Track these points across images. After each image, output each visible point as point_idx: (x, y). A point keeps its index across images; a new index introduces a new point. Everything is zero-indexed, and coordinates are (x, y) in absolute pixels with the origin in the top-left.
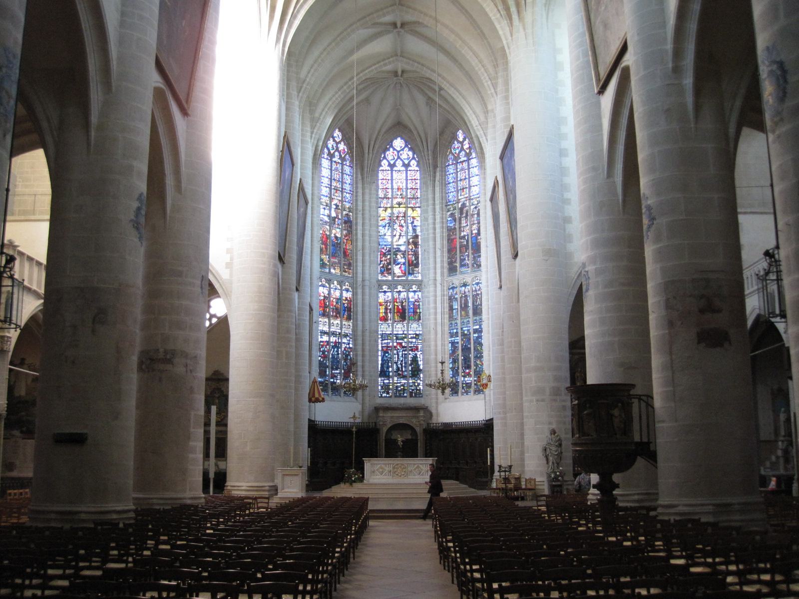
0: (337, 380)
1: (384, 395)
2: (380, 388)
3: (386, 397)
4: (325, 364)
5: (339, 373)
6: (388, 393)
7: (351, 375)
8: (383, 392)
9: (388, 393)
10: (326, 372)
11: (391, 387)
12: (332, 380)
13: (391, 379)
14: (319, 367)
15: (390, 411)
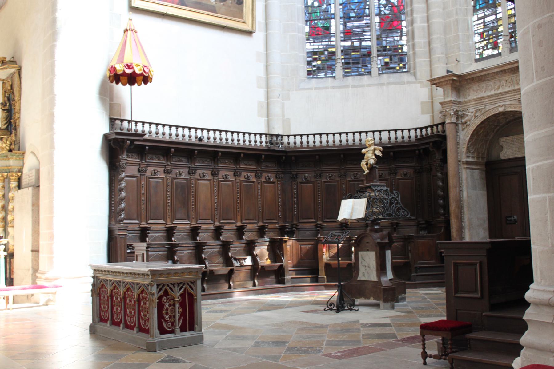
0: (361, 41)
1: (489, 52)
2: (477, 38)
3: (492, 56)
4: (326, 11)
5: (368, 25)
6: (495, 46)
7: (404, 24)
8: (485, 48)
9: (495, 46)
10: (328, 28)
11: (501, 29)
12: (348, 43)
13: (499, 9)
14: (309, 20)
15: (475, 87)
